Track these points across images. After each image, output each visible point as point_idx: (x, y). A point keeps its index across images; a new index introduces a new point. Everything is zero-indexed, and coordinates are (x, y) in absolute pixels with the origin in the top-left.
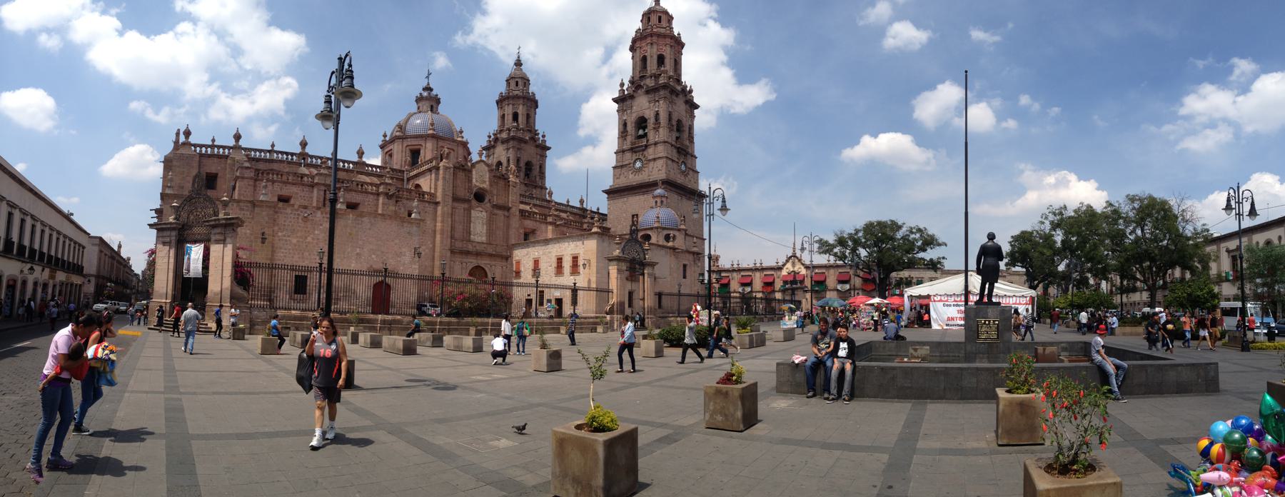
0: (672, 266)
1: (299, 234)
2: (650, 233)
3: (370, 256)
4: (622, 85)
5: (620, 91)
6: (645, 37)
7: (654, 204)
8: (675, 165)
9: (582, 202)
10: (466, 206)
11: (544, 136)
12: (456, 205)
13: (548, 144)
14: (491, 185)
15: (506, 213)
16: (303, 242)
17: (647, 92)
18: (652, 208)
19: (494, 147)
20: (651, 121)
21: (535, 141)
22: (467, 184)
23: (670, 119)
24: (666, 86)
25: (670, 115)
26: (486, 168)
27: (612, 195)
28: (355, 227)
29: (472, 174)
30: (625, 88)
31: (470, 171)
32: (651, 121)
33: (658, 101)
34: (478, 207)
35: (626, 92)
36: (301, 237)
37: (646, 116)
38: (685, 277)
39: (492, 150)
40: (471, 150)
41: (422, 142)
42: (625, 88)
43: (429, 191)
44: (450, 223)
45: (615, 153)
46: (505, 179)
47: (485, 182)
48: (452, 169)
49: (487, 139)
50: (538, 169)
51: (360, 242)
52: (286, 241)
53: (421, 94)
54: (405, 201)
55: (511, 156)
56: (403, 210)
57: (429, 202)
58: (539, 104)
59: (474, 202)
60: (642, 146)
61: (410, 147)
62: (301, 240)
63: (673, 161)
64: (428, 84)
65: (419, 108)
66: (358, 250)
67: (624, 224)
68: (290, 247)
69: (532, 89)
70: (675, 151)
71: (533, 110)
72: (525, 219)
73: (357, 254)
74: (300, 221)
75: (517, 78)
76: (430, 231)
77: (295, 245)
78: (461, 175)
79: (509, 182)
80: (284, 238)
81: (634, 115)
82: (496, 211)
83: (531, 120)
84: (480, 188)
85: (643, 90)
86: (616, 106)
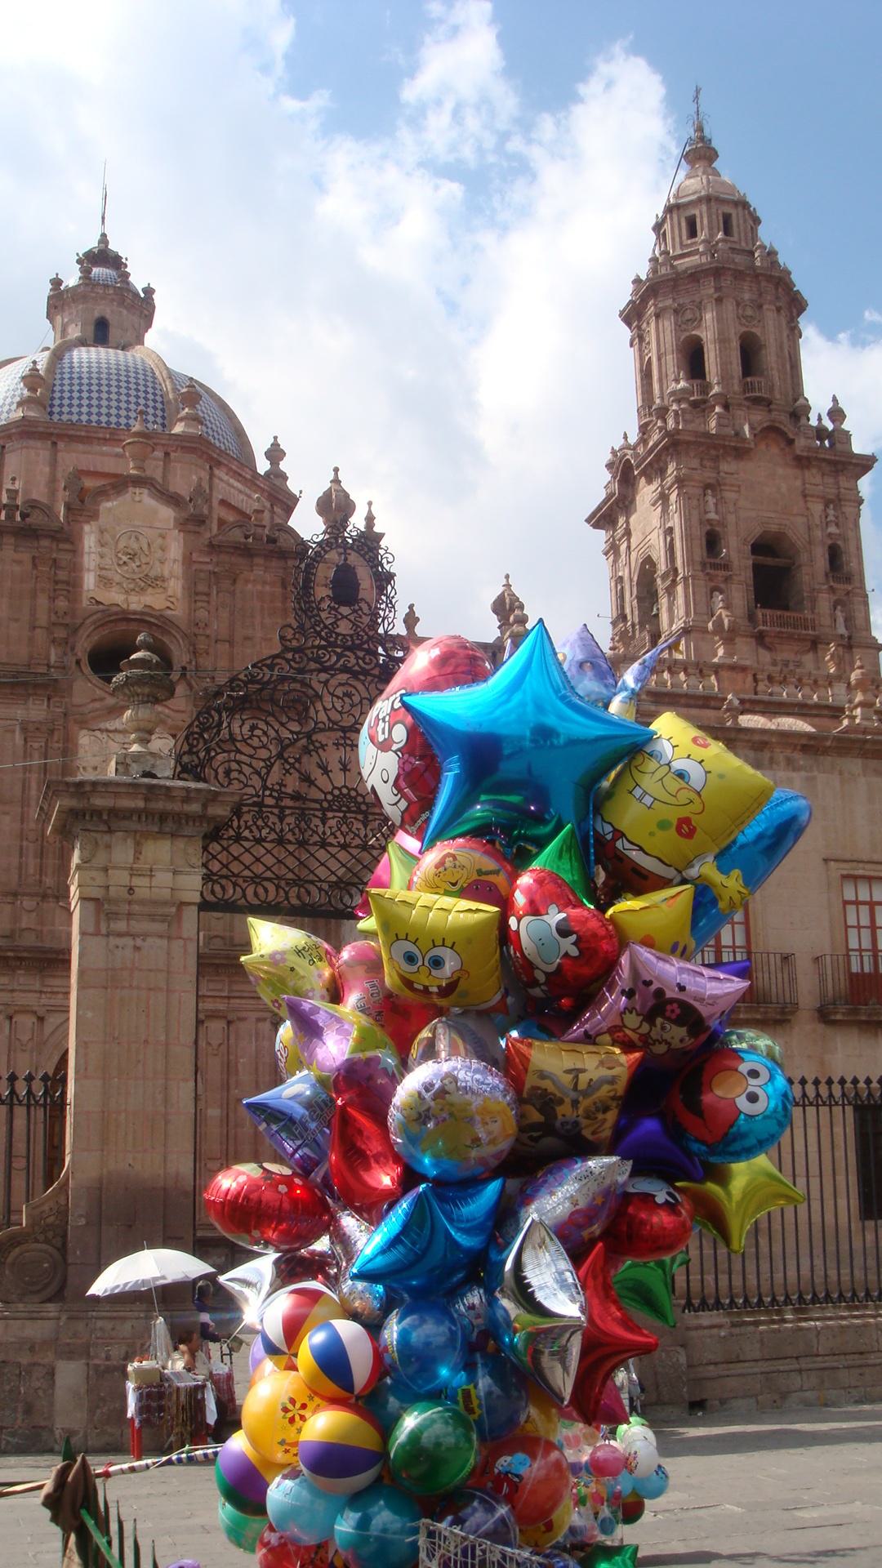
10: (36, 710)
13: (858, 447)
14: (194, 593)
21: (790, 442)
22: (43, 601)
26: (167, 514)
29: (76, 551)
31: (67, 538)
47: (155, 582)
50: (821, 562)
55: (675, 521)
58: (801, 282)
59: (85, 689)
71: (770, 316)
75: (690, 203)
83: (770, 358)
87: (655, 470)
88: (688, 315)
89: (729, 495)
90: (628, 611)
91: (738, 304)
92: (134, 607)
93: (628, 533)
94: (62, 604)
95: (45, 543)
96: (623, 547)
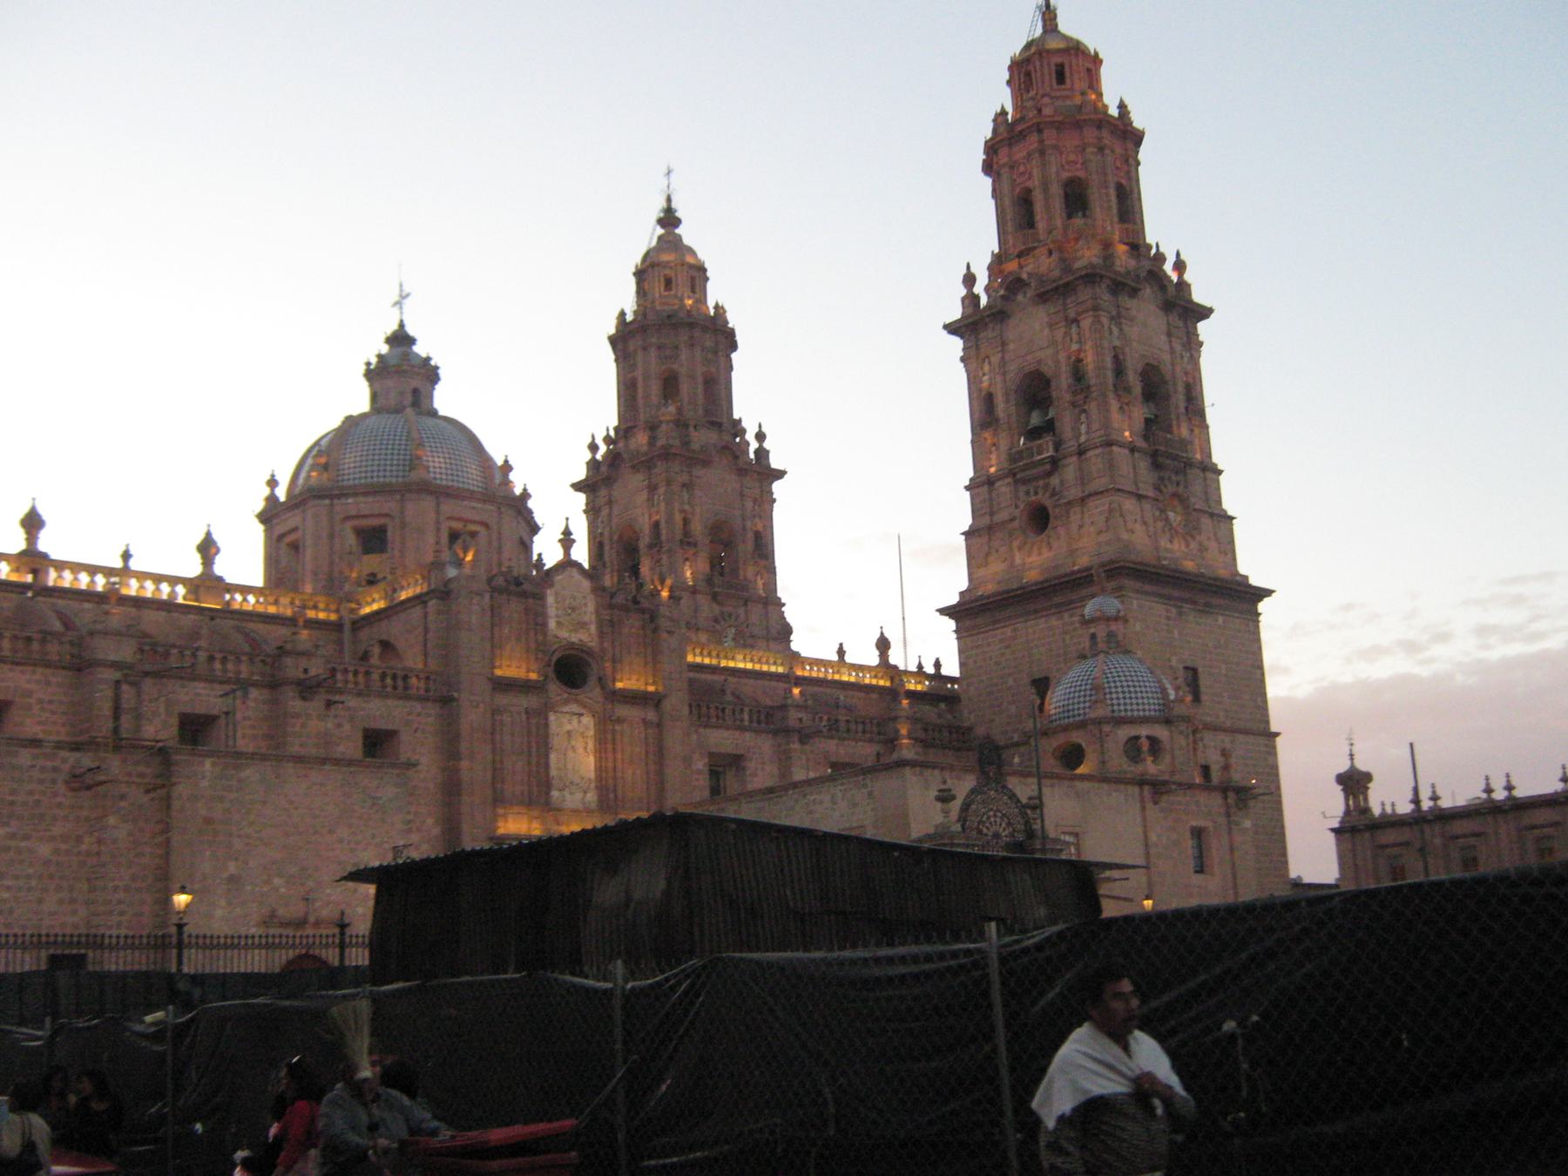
0: (1153, 838)
1: (57, 830)
2: (1079, 740)
3: (268, 882)
4: (969, 280)
5: (963, 299)
6: (1022, 135)
7: (1087, 643)
8: (1147, 506)
9: (883, 645)
10: (531, 701)
11: (760, 436)
12: (503, 700)
14: (601, 635)
15: (651, 715)
16: (68, 852)
17: (1043, 298)
18: (1084, 657)
19: (609, 481)
20: (1064, 381)
22: (532, 633)
23: (1119, 371)
24: (1094, 275)
25: (1116, 357)
27: (968, 623)
28: (221, 799)
29: (544, 606)
30: (979, 288)
31: (541, 598)
32: (1064, 381)
33: (1076, 321)
34: (566, 702)
35: (984, 301)
36: (65, 838)
37: (1047, 369)
38: (1200, 870)
39: (603, 492)
40: (539, 518)
41: (390, 505)
42: (979, 288)
43: (420, 666)
44: (490, 757)
45: (967, 488)
46: (643, 611)
47: (582, 625)
48: (487, 596)
49: (588, 456)
50: (750, 546)
51: (238, 844)
52: (19, 851)
53: (380, 356)
54: (352, 702)
56: (347, 727)
57: (423, 699)
58: (739, 338)
59: (554, 688)
60: (1041, 462)
61: (357, 522)
62: (63, 847)
63: (1140, 497)
64: (402, 325)
65: (374, 397)
66: (232, 868)
67: (1013, 709)
68: (31, 871)
69: (715, 294)
70: (1144, 465)
72: (706, 726)
73: (231, 879)
74: (61, 787)
76: (431, 785)
77: (47, 863)
78: (513, 609)
79: (653, 618)
80: (13, 843)
81: (1013, 367)
82: (623, 711)
84: (571, 646)
85: (1030, 293)
86: (956, 344)
87: (645, 464)
88: (668, 352)
89: (698, 493)
90: (607, 559)
91: (703, 350)
92: (574, 640)
93: (610, 503)
94: (540, 638)
95: (530, 600)
96: (605, 512)
